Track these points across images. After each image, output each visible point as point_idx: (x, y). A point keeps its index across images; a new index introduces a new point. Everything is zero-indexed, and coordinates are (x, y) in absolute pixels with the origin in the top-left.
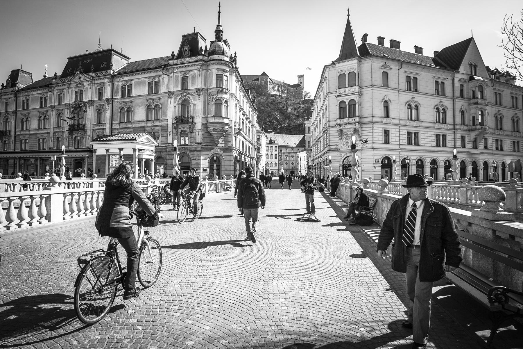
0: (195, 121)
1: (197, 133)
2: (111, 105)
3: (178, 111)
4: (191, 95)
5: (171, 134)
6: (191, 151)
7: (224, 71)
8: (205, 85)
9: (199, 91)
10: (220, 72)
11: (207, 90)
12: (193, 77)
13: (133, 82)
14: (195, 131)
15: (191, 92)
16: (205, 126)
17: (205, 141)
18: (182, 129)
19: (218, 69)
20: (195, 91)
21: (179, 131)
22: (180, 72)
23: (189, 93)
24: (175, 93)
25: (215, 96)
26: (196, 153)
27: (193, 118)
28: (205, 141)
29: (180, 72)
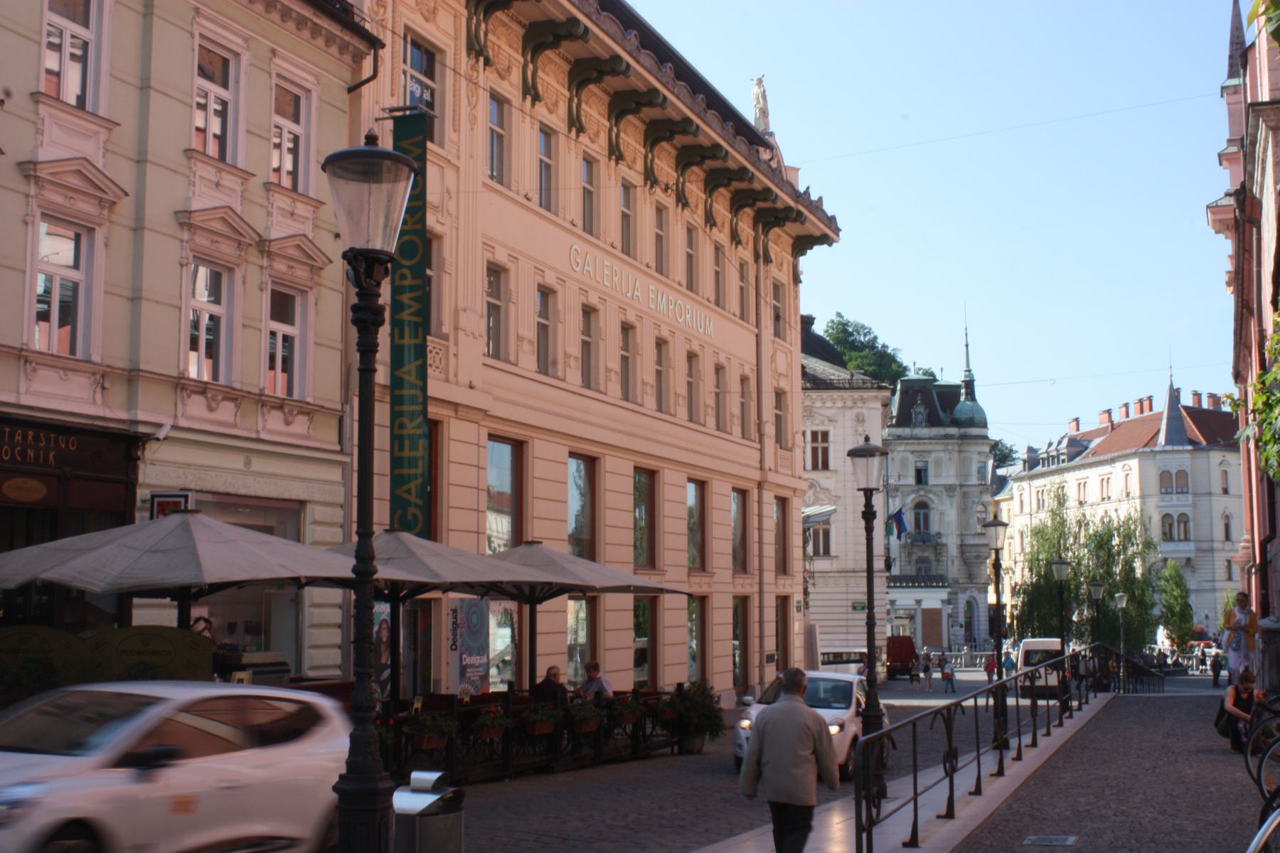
0: (944, 540)
4: (935, 494)
9: (950, 489)
11: (961, 486)
12: (938, 463)
15: (934, 489)
18: (920, 554)
20: (942, 488)
21: (914, 557)
22: (912, 452)
23: (930, 492)
24: (902, 489)
29: (912, 452)
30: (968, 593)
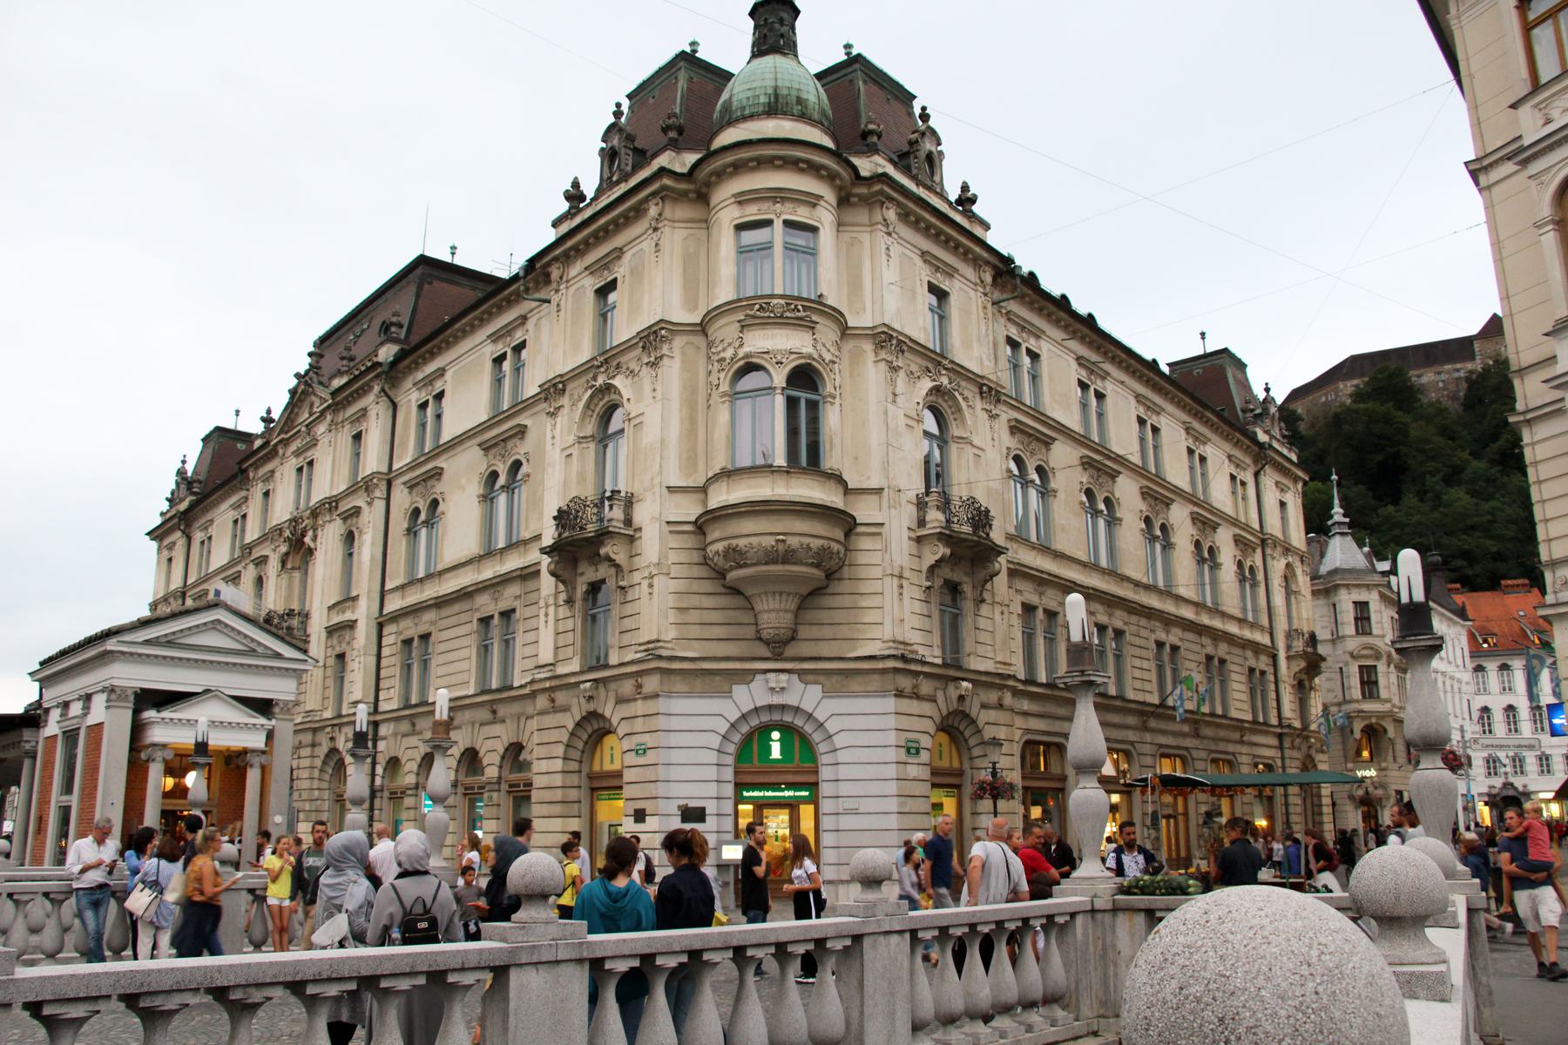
1: (645, 583)
2: (380, 505)
3: (582, 477)
5: (551, 610)
6: (621, 701)
7: (778, 196)
8: (691, 302)
10: (752, 213)
13: (449, 375)
14: (637, 577)
16: (690, 541)
17: (696, 631)
19: (742, 199)
25: (728, 354)
26: (639, 707)
27: (629, 502)
28: (696, 631)
30: (748, 696)
